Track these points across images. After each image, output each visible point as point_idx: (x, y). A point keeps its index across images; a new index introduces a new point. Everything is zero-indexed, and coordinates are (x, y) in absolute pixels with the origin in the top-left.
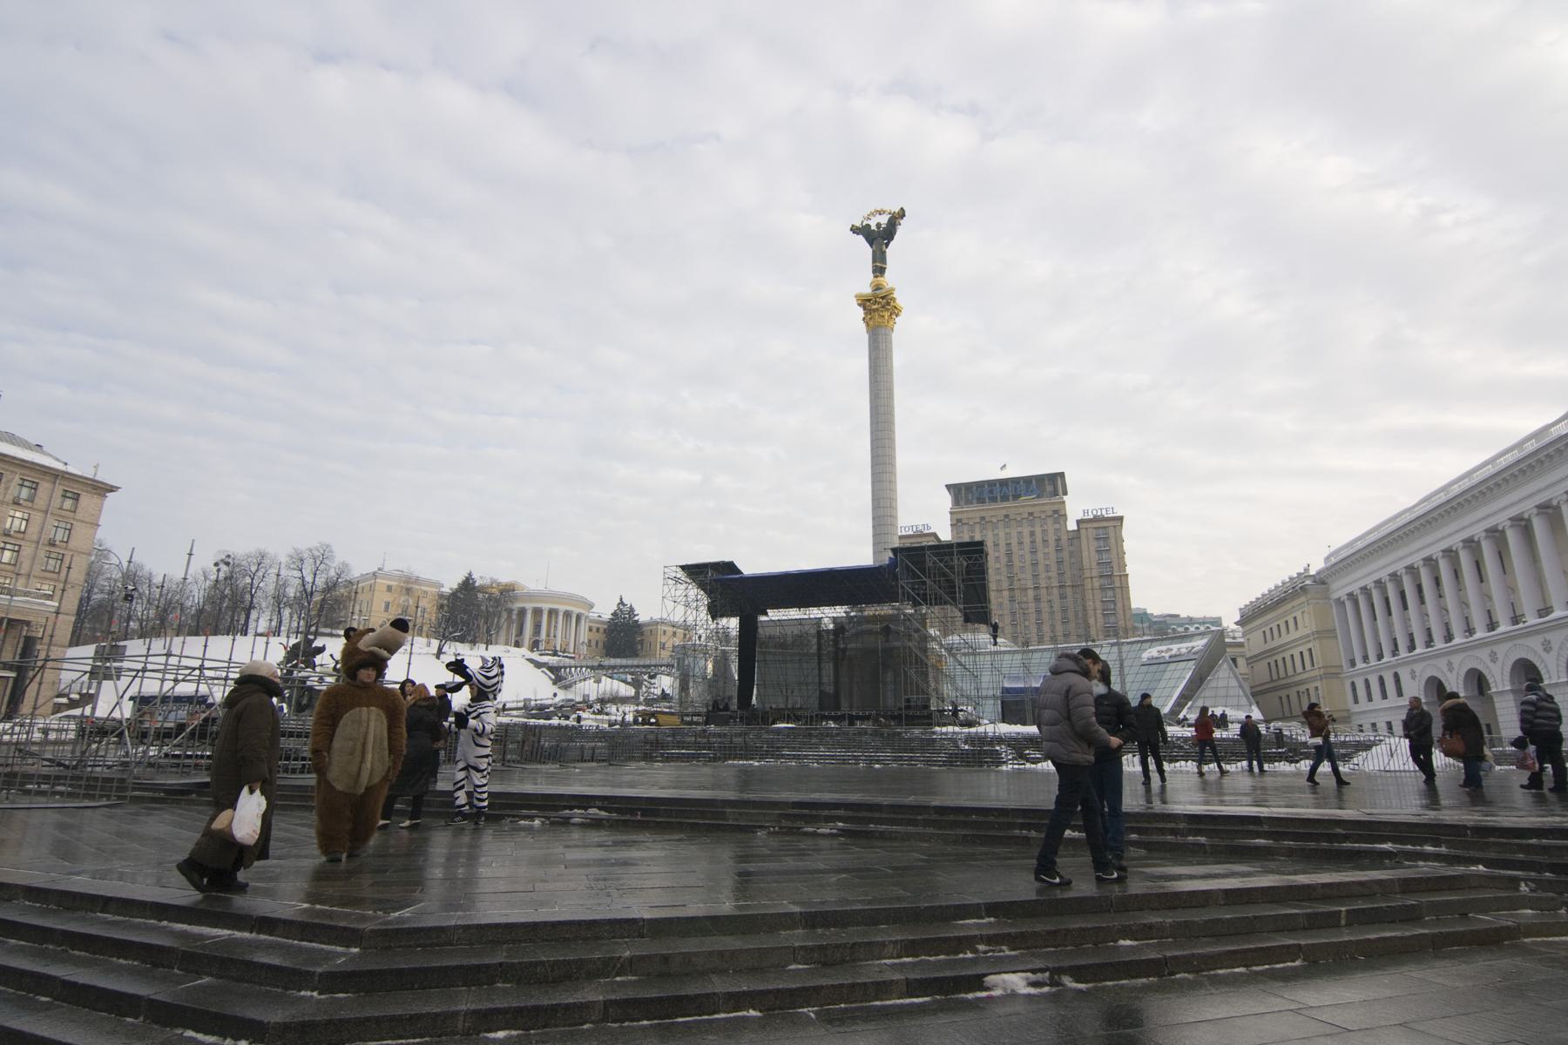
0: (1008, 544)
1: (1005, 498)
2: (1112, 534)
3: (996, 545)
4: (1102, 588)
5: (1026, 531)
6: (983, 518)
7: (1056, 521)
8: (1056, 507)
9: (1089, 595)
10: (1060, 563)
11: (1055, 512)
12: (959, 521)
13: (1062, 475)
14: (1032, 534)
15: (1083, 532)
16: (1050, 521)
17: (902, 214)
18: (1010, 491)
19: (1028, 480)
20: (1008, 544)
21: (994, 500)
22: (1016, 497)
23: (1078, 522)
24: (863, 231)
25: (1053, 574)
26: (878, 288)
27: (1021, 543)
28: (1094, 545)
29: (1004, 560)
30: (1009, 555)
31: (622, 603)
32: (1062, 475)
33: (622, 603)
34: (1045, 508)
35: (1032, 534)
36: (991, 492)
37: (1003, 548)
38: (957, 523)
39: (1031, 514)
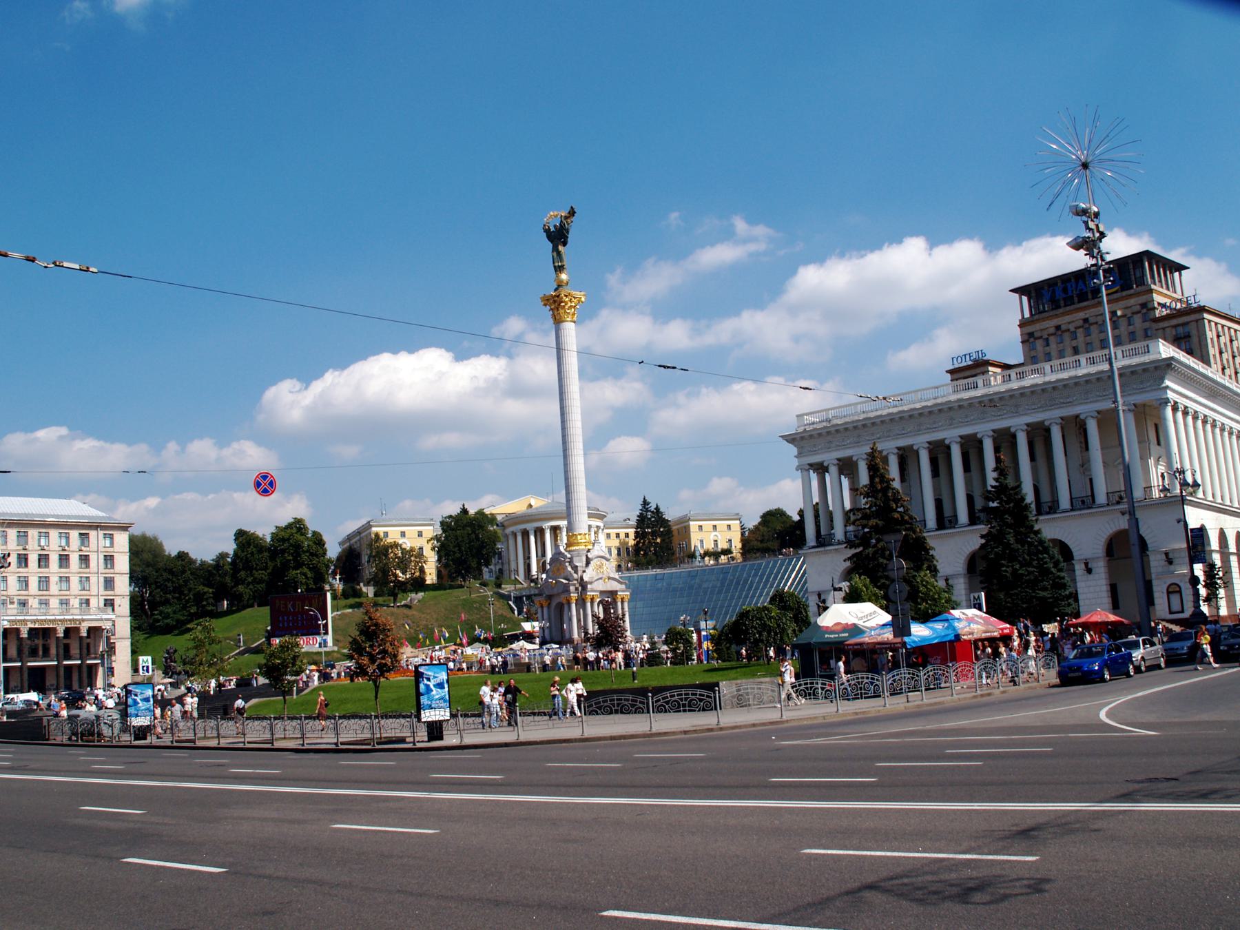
1: (1083, 297)
2: (1194, 332)
6: (1058, 328)
8: (1142, 299)
11: (1144, 305)
12: (1031, 335)
17: (572, 213)
21: (1069, 301)
24: (547, 231)
26: (560, 286)
31: (645, 503)
33: (645, 503)
34: (1132, 301)
36: (1065, 290)
38: (1028, 339)
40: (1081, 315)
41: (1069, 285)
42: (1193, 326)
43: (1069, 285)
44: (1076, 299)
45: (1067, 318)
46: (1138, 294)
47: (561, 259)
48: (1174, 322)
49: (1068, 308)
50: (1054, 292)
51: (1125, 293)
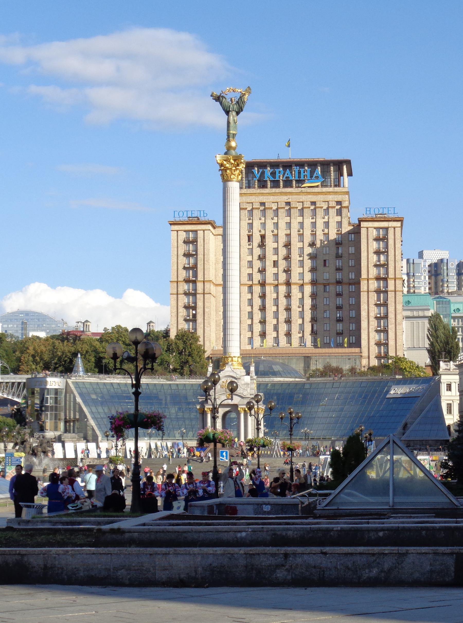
0: (288, 236)
1: (288, 183)
3: (276, 236)
4: (378, 292)
5: (308, 221)
6: (263, 204)
7: (339, 213)
9: (364, 296)
10: (338, 256)
13: (348, 163)
14: (314, 225)
15: (363, 231)
16: (332, 212)
18: (293, 175)
19: (313, 165)
20: (288, 236)
21: (276, 184)
22: (300, 182)
23: (360, 221)
25: (331, 268)
27: (301, 236)
28: (374, 246)
29: (283, 252)
30: (288, 245)
32: (348, 163)
35: (314, 225)
36: (273, 174)
37: (282, 240)
39: (313, 203)
40: (285, 198)
41: (277, 171)
42: (391, 231)
43: (277, 171)
44: (281, 184)
45: (272, 198)
46: (336, 193)
47: (235, 128)
48: (377, 224)
49: (274, 190)
50: (263, 173)
51: (324, 190)
